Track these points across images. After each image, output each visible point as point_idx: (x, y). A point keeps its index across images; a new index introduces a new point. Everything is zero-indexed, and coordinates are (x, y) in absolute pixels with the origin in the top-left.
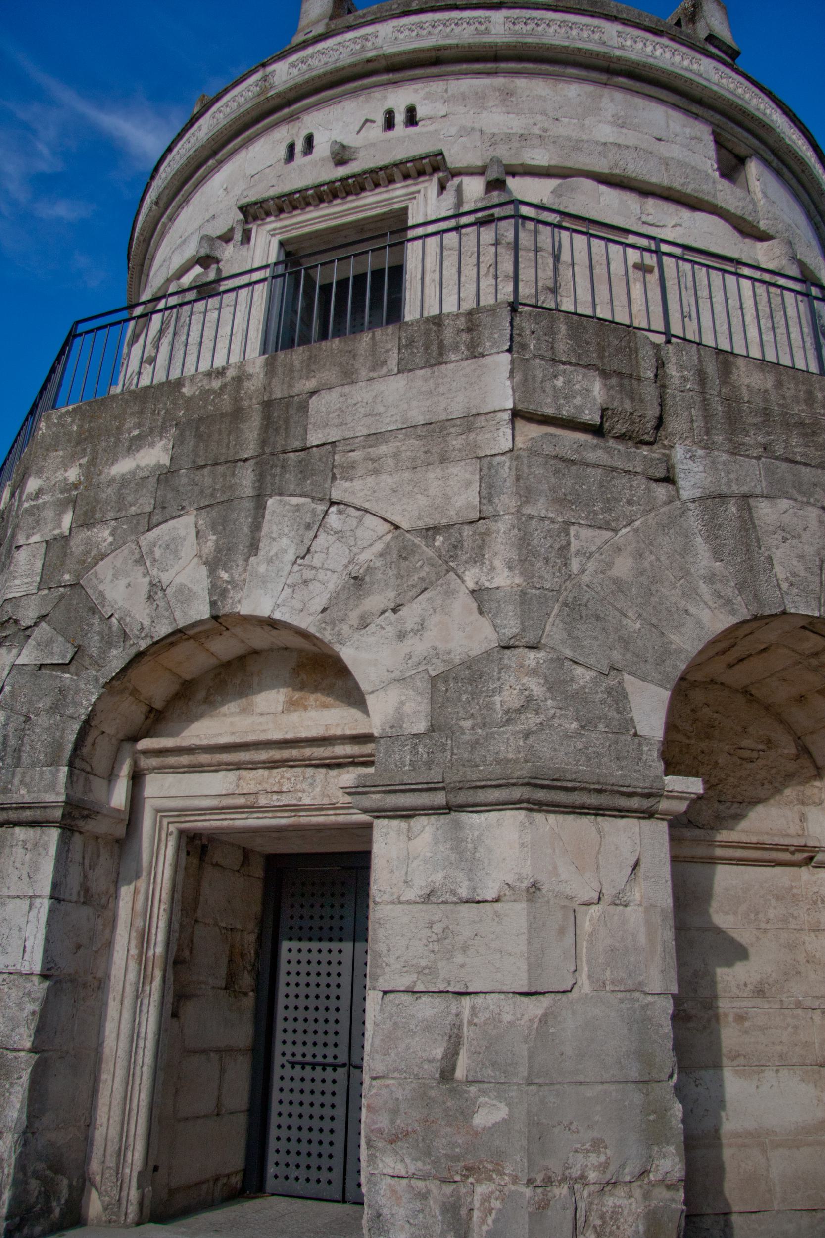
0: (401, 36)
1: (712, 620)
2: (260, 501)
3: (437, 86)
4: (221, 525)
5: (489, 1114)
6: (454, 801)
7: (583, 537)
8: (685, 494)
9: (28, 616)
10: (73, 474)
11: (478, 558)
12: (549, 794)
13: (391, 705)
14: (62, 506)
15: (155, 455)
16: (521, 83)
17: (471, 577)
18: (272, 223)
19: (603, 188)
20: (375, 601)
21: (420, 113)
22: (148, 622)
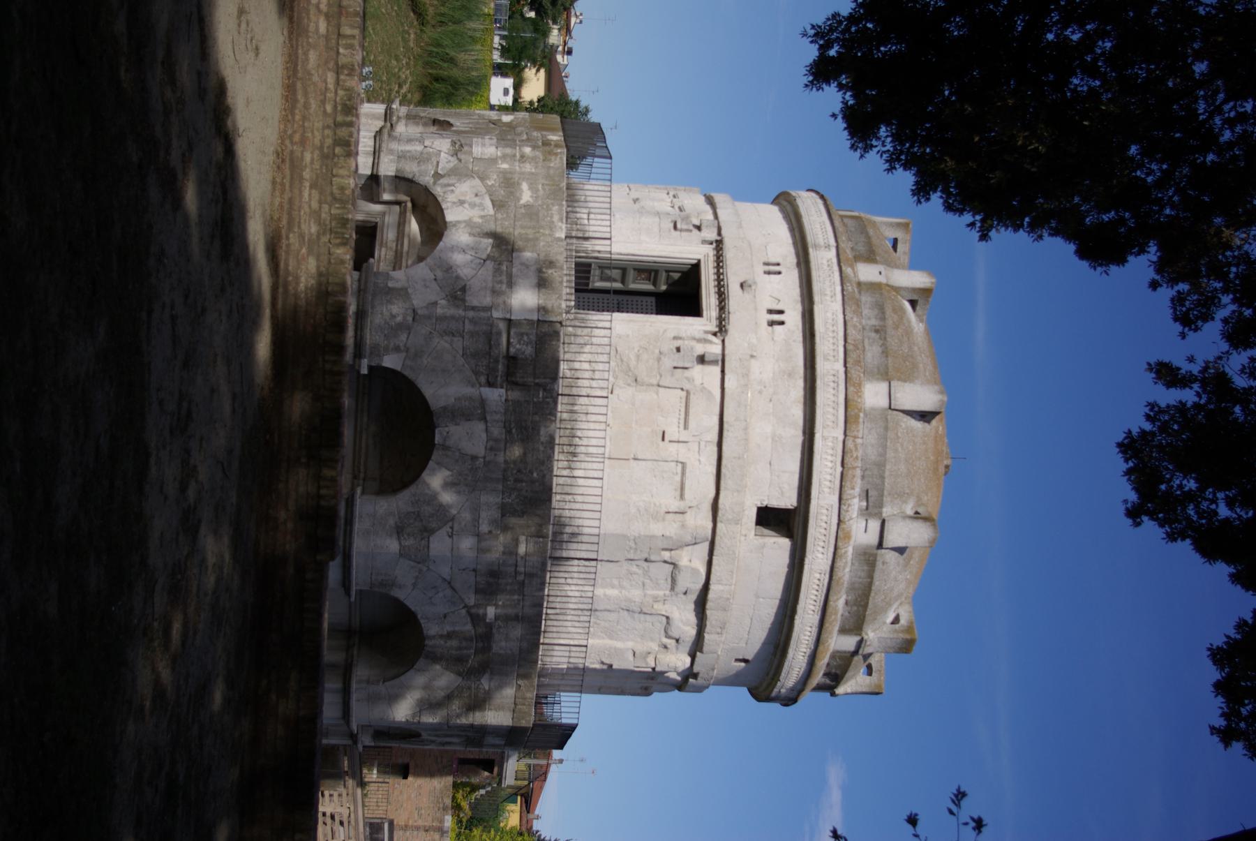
0: (829, 315)
8: (482, 389)
15: (526, 196)
16: (800, 383)
17: (443, 302)
20: (439, 274)
21: (777, 328)
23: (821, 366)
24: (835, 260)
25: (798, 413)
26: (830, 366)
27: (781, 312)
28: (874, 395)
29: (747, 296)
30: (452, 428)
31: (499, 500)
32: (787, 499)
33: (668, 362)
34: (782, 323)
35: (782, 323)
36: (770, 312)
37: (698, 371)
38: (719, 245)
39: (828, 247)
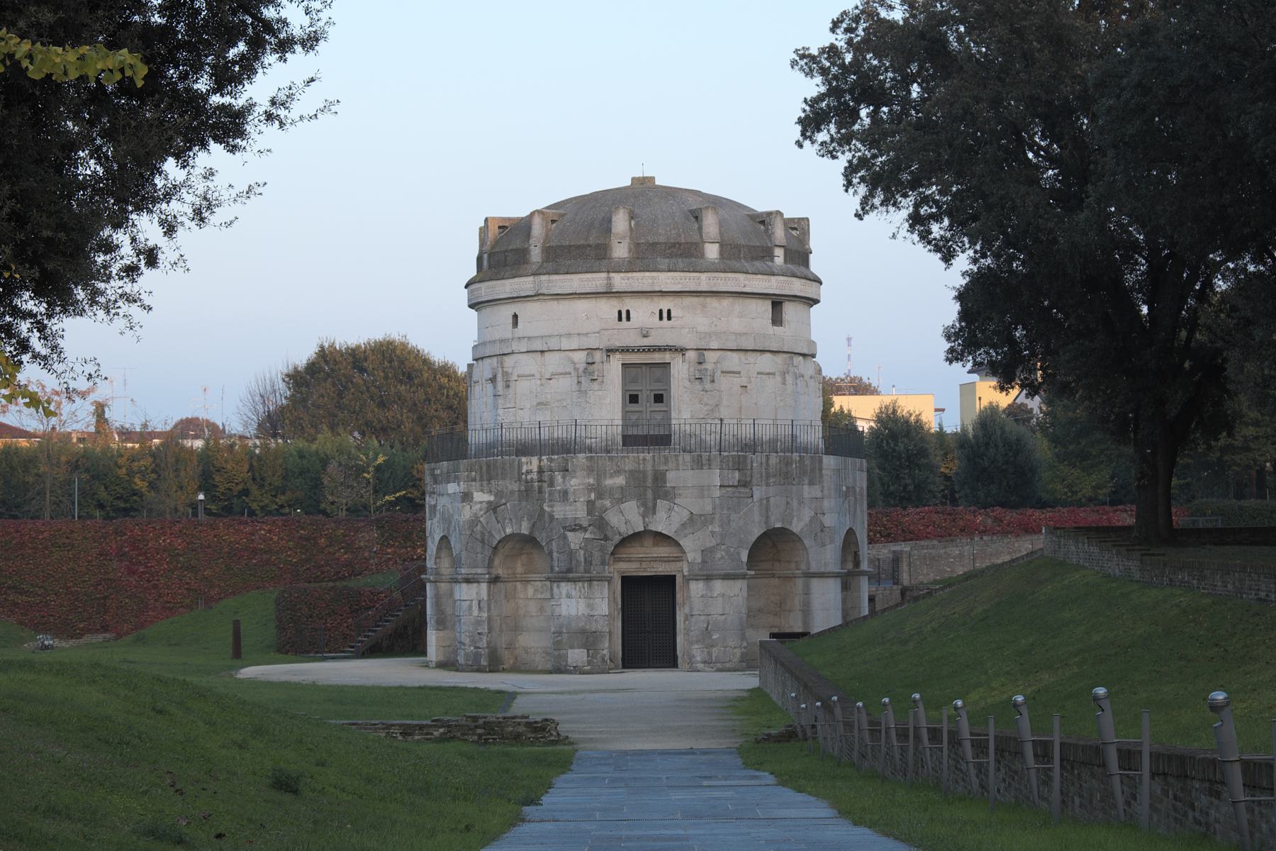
1: (757, 532)
2: (655, 500)
3: (678, 301)
4: (644, 505)
5: (715, 637)
6: (708, 578)
7: (734, 516)
9: (585, 524)
10: (591, 481)
11: (712, 523)
12: (727, 577)
13: (693, 555)
14: (590, 491)
15: (620, 480)
16: (708, 300)
18: (618, 356)
19: (735, 354)
22: (626, 530)
23: (704, 287)
24: (622, 275)
25: (726, 302)
26: (704, 281)
27: (661, 311)
28: (712, 252)
29: (653, 332)
30: (772, 519)
31: (806, 487)
32: (767, 305)
33: (708, 386)
34: (669, 311)
35: (669, 311)
36: (661, 318)
37: (709, 366)
38: (610, 351)
39: (609, 278)
